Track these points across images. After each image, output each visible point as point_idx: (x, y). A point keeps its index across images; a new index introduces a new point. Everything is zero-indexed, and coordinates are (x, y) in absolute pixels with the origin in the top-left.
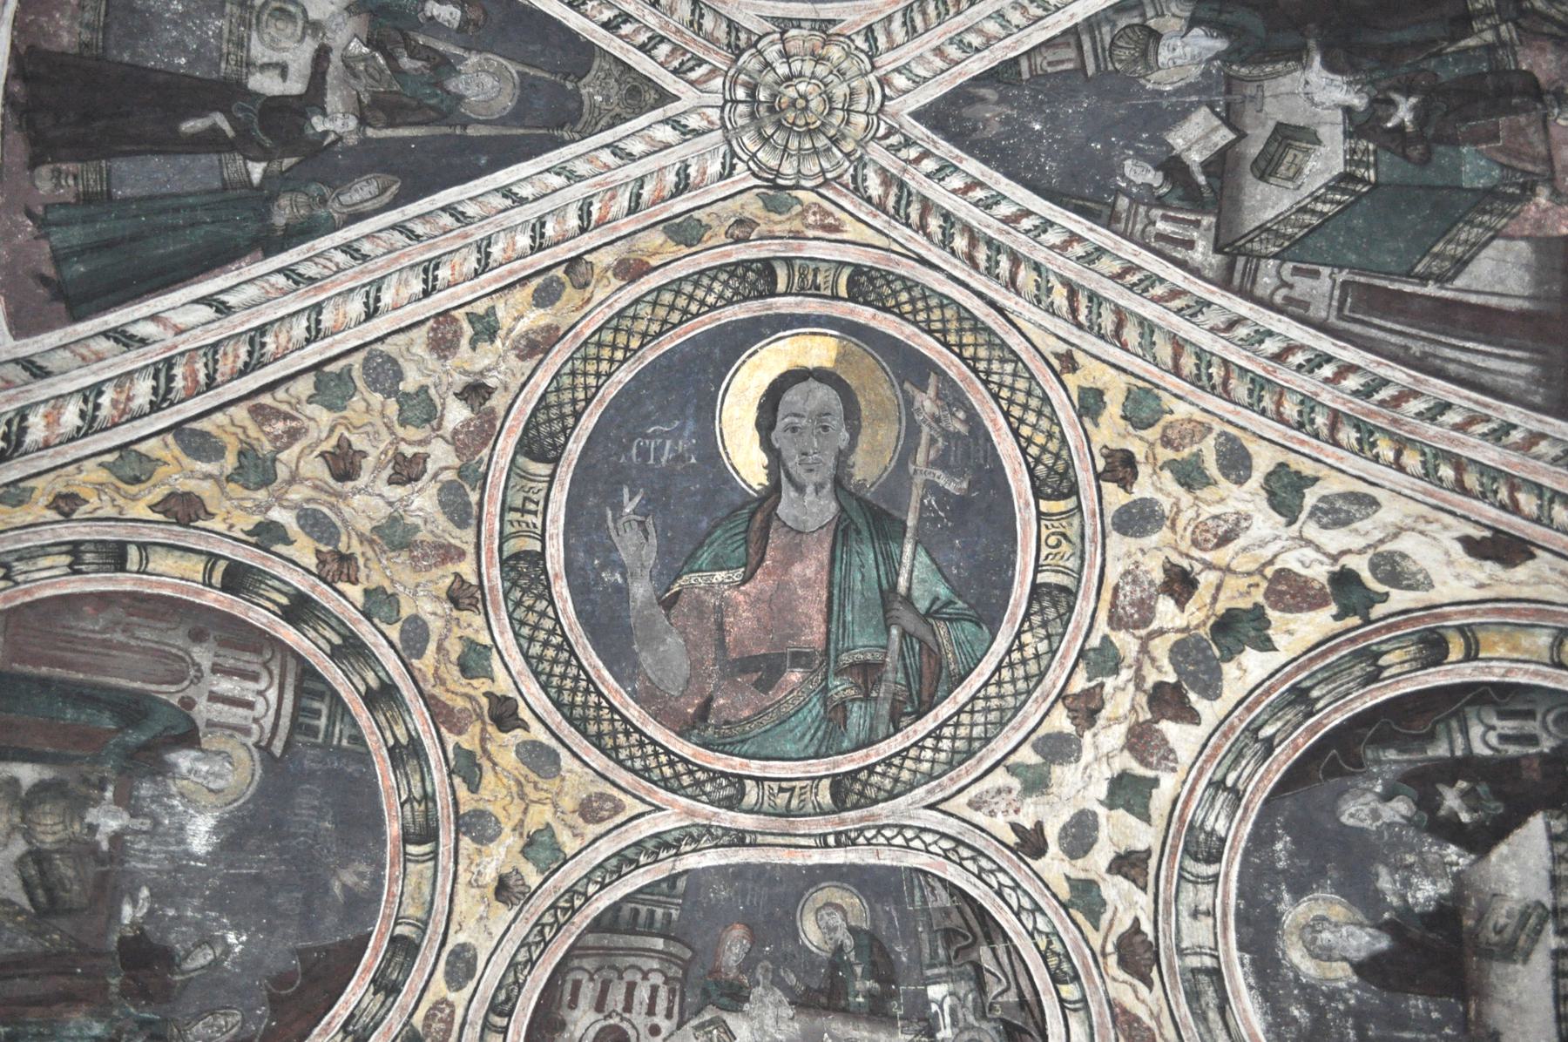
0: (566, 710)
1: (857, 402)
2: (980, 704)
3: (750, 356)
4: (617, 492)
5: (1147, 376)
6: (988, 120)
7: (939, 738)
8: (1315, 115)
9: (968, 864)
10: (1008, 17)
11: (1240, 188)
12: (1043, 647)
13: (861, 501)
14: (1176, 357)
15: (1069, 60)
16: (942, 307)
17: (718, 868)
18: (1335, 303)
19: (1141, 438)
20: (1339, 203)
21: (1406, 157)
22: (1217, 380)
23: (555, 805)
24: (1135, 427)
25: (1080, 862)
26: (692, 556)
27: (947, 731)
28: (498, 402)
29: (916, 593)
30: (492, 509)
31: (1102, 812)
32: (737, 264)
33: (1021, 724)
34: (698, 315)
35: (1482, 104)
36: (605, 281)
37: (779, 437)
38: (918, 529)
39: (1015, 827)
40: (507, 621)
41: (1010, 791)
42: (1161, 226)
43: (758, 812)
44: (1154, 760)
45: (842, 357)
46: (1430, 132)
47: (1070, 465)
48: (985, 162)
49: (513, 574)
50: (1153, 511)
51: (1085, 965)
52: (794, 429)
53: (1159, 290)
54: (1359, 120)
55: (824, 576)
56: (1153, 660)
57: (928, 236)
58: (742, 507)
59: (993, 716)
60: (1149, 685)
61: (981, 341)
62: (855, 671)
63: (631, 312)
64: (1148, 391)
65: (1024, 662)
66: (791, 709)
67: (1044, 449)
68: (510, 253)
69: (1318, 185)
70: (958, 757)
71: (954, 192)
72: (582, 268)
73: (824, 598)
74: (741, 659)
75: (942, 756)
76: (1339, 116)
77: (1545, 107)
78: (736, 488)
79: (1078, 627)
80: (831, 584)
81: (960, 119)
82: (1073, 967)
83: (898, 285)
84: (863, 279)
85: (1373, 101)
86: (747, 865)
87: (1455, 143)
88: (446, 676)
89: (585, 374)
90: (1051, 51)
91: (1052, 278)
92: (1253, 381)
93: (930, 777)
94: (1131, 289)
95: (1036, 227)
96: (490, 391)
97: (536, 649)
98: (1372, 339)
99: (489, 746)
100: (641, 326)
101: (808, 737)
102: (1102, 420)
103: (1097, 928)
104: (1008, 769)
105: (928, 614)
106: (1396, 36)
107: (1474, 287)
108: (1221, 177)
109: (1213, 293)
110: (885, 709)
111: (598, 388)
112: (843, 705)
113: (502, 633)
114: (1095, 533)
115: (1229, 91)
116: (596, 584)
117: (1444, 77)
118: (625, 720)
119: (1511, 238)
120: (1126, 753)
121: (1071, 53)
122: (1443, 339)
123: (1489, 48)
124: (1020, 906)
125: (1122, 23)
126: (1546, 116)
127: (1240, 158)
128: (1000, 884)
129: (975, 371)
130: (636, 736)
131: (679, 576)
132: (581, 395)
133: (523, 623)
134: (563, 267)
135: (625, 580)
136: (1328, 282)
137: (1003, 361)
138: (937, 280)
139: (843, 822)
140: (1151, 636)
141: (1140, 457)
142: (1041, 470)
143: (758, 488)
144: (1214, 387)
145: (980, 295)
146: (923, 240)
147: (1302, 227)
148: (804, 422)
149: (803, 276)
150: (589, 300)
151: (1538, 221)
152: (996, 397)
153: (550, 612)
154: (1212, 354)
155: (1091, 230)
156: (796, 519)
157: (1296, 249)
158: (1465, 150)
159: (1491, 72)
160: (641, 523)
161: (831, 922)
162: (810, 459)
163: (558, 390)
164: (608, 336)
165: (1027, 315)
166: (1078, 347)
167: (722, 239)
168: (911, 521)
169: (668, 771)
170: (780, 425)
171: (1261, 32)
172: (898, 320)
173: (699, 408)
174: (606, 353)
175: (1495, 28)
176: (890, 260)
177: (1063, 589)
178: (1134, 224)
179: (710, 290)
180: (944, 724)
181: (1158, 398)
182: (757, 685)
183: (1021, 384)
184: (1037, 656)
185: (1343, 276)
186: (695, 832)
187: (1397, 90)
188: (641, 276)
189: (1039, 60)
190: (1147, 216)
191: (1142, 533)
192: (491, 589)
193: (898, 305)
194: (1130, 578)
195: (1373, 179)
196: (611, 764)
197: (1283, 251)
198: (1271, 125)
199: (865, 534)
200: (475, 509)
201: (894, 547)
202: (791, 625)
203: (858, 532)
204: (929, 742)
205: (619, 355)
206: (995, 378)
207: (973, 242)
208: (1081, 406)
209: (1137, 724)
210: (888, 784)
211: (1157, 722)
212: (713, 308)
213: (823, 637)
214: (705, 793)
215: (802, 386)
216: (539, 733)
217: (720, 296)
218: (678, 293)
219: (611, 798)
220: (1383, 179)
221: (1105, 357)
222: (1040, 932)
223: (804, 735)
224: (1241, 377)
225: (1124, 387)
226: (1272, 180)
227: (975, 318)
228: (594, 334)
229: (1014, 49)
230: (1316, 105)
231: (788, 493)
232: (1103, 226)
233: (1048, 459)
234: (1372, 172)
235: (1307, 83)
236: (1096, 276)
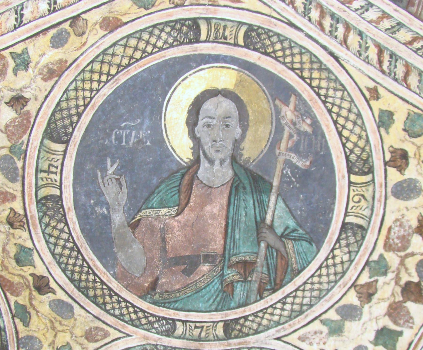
0: (76, 283)
1: (247, 111)
2: (308, 286)
3: (183, 80)
4: (104, 162)
7: (284, 303)
12: (346, 258)
13: (246, 170)
16: (301, 54)
19: (413, 143)
23: (72, 333)
24: (410, 136)
26: (147, 199)
27: (289, 300)
28: (32, 107)
29: (276, 224)
30: (31, 171)
31: (370, 347)
32: (176, 21)
33: (330, 298)
34: (152, 53)
36: (95, 31)
37: (199, 130)
38: (280, 187)
40: (41, 235)
41: (321, 333)
43: (183, 338)
44: (401, 322)
45: (239, 83)
47: (370, 155)
49: (44, 208)
50: (415, 186)
52: (209, 126)
55: (224, 213)
56: (406, 269)
57: (295, 8)
58: (177, 172)
59: (315, 293)
60: (403, 282)
61: (323, 76)
62: (239, 266)
63: (110, 51)
65: (335, 265)
66: (202, 285)
67: (356, 145)
68: (35, 14)
70: (294, 314)
72: (80, 23)
73: (223, 225)
74: (175, 258)
75: (286, 313)
78: (174, 160)
79: (366, 248)
80: (227, 217)
83: (275, 39)
84: (254, 34)
88: (8, 265)
89: (83, 90)
91: (370, 43)
93: (278, 323)
94: (416, 52)
95: (362, 7)
96: (26, 101)
97: (58, 250)
99: (34, 302)
100: (117, 60)
101: (212, 300)
102: (391, 130)
104: (321, 321)
105: (282, 236)
110: (255, 286)
111: (91, 98)
112: (232, 284)
113: (39, 241)
114: (381, 196)
116: (93, 213)
118: (110, 289)
120: (387, 317)
129: (318, 95)
130: (116, 297)
131: (140, 211)
132: (81, 102)
133: (50, 236)
134: (69, 22)
135: (109, 212)
137: (335, 90)
140: (407, 256)
141: (411, 154)
142: (353, 157)
143: (186, 160)
145: (325, 48)
146: (292, 11)
148: (215, 121)
149: (217, 30)
150: (85, 43)
152: (330, 111)
153: (66, 229)
156: (208, 178)
160: (117, 180)
162: (218, 144)
163: (67, 99)
164: (97, 66)
165: (352, 63)
166: (381, 85)
167: (168, 5)
168: (275, 183)
169: (133, 316)
170: (201, 123)
172: (274, 61)
173: (152, 112)
174: (96, 77)
176: (271, 22)
177: (360, 227)
179: (159, 37)
180: (288, 296)
182: (183, 272)
183: (346, 105)
184: (342, 263)
188: (116, 28)
191: (408, 198)
192: (32, 217)
193: (274, 52)
194: (398, 223)
196: (102, 312)
199: (248, 189)
200: (20, 171)
201: (265, 197)
202: (204, 240)
203: (244, 188)
204: (279, 305)
205: (104, 78)
206: (330, 100)
207: (323, 14)
208: (380, 121)
209: (394, 302)
210: (255, 326)
211: (405, 302)
212: (161, 49)
213: (222, 247)
214: (154, 328)
215: (214, 100)
216: (61, 295)
217: (166, 42)
218: (140, 39)
219: (102, 330)
221: (396, 92)
223: (209, 300)
225: (406, 112)
227: (321, 63)
228: (88, 65)
231: (204, 164)
232: (403, 8)
233: (357, 151)
236: (396, 42)
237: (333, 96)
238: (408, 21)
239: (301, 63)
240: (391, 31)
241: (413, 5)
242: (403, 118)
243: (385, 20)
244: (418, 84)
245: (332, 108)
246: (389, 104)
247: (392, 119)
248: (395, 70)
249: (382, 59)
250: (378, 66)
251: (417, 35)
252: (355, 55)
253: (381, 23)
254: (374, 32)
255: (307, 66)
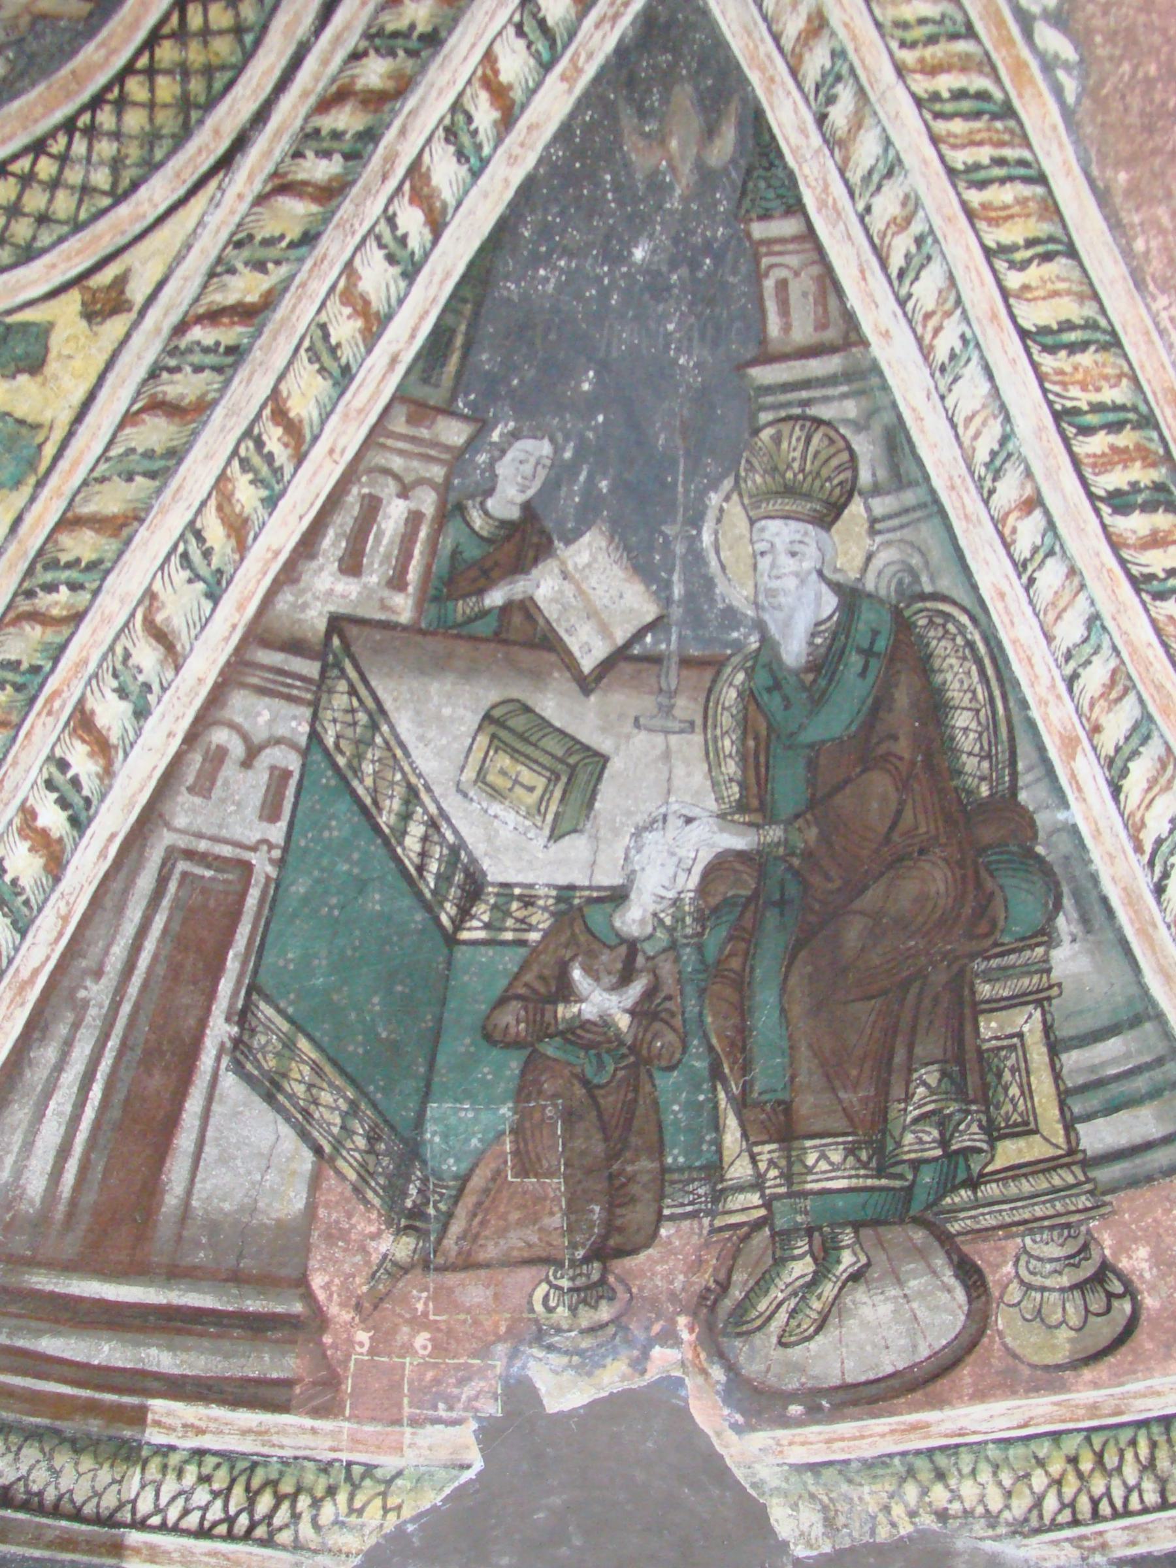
5: (63, 465)
6: (663, 143)
8: (616, 832)
10: (887, 186)
11: (469, 673)
14: (98, 523)
15: (787, 328)
16: (238, 30)
18: (203, 846)
20: (420, 869)
21: (502, 1001)
22: (44, 601)
35: (598, 1147)
42: (394, 513)
46: (550, 1049)
48: (564, 133)
53: (246, 495)
54: (595, 915)
61: (161, 117)
64: (32, 465)
69: (464, 832)
71: (489, 57)
76: (608, 878)
77: (573, 1264)
81: (667, 79)
85: (632, 946)
87: (524, 1091)
90: (812, 287)
92: (35, 670)
94: (248, 433)
95: (403, 241)
98: (120, 910)
106: (766, 999)
107: (215, 1107)
108: (499, 638)
109: (241, 607)
115: (686, 662)
117: (666, 1082)
119: (315, 1182)
121: (803, 332)
122: (113, 1043)
123: (714, 1170)
125: (865, 447)
126: (559, 1264)
127: (538, 677)
129: (96, 103)
136: (253, 837)
137: (116, 164)
138: (297, 19)
144: (30, 594)
145: (261, 116)
147: (374, 792)
151: (344, 1235)
152: (38, 148)
154: (96, 593)
155: (394, 360)
157: (328, 779)
158: (505, 1110)
159: (664, 1170)
165: (213, 220)
166: (135, 325)
171: (811, 735)
175: (758, 1184)
178: (401, 453)
181: (17, 483)
185: (263, 866)
187: (649, 994)
189: (793, 261)
190: (421, 482)
195: (465, 935)
197: (326, 751)
198: (604, 744)
206: (80, 147)
208: (9, 328)
220: (462, 955)
221: (111, 378)
224: (45, 647)
225: (47, 417)
226: (483, 740)
227: (210, 104)
229: (822, 205)
230: (638, 834)
232: (399, 387)
234: (481, 935)
235: (689, 820)
236: (280, 362)
237: (95, 158)
238: (358, 403)
239: (206, 33)
240: (320, 345)
241: (411, 420)
242: (21, 410)
243: (359, 323)
244: (140, 450)
245: (51, 155)
246: (70, 357)
247: (20, 371)
248: (188, 369)
249: (226, 320)
250: (201, 311)
251: (308, 437)
252: (239, 225)
253: (348, 311)
254: (313, 285)
255: (195, 55)
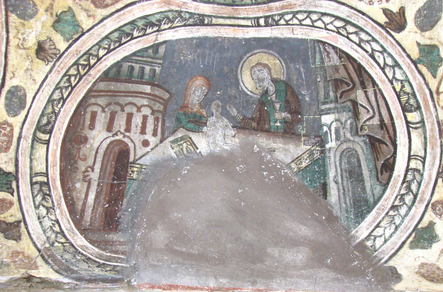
9: (353, 37)
17: (186, 40)
25: (427, 34)
39: (386, 12)
51: (425, 100)
82: (417, 101)
86: (206, 39)
103: (435, 77)
124: (385, 64)
128: (373, 50)
139: (270, 9)
161: (261, 76)
186: (170, 15)
222: (397, 80)
